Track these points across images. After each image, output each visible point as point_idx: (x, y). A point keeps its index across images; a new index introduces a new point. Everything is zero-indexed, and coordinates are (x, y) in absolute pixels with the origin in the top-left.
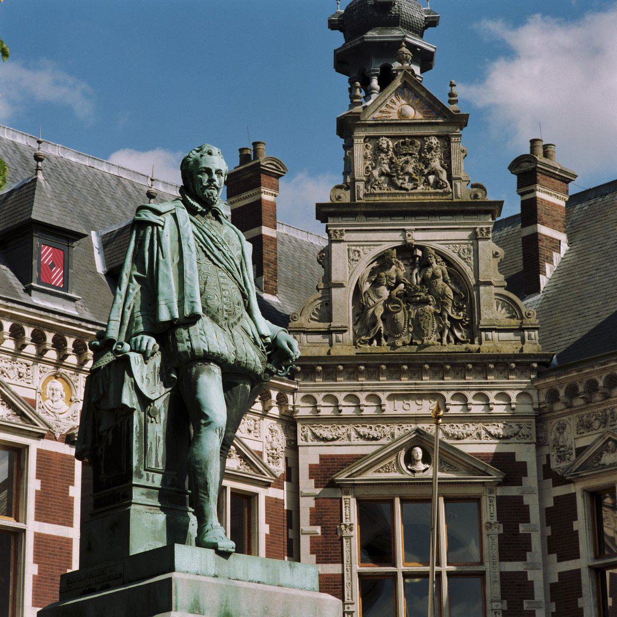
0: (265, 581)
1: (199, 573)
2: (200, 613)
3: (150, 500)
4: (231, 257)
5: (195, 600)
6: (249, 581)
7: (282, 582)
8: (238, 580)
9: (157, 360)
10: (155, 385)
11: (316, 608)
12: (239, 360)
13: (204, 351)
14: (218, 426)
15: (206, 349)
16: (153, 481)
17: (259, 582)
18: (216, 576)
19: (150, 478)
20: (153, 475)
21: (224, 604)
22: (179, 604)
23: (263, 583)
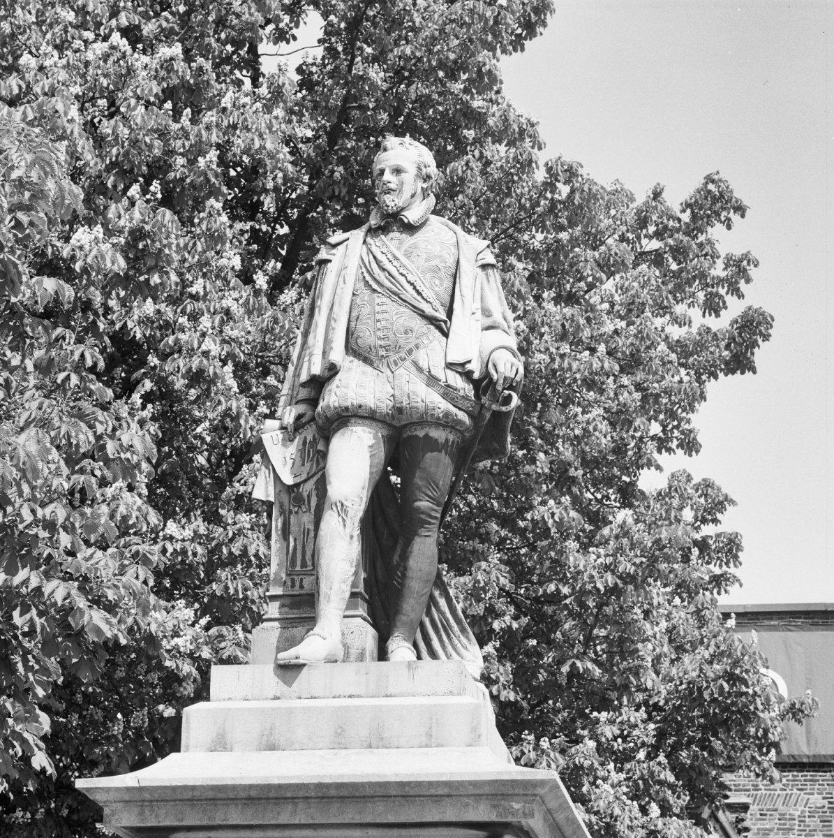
0: (362, 693)
1: (249, 697)
2: (225, 749)
3: (295, 611)
4: (401, 274)
5: (218, 734)
6: (334, 697)
7: (391, 690)
8: (315, 698)
9: (309, 433)
10: (303, 465)
11: (431, 719)
12: (398, 405)
13: (335, 408)
14: (334, 501)
15: (336, 404)
16: (301, 587)
17: (350, 696)
18: (276, 698)
19: (297, 584)
20: (302, 580)
21: (266, 733)
22: (191, 744)
23: (359, 696)
